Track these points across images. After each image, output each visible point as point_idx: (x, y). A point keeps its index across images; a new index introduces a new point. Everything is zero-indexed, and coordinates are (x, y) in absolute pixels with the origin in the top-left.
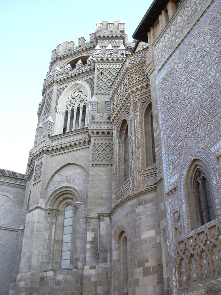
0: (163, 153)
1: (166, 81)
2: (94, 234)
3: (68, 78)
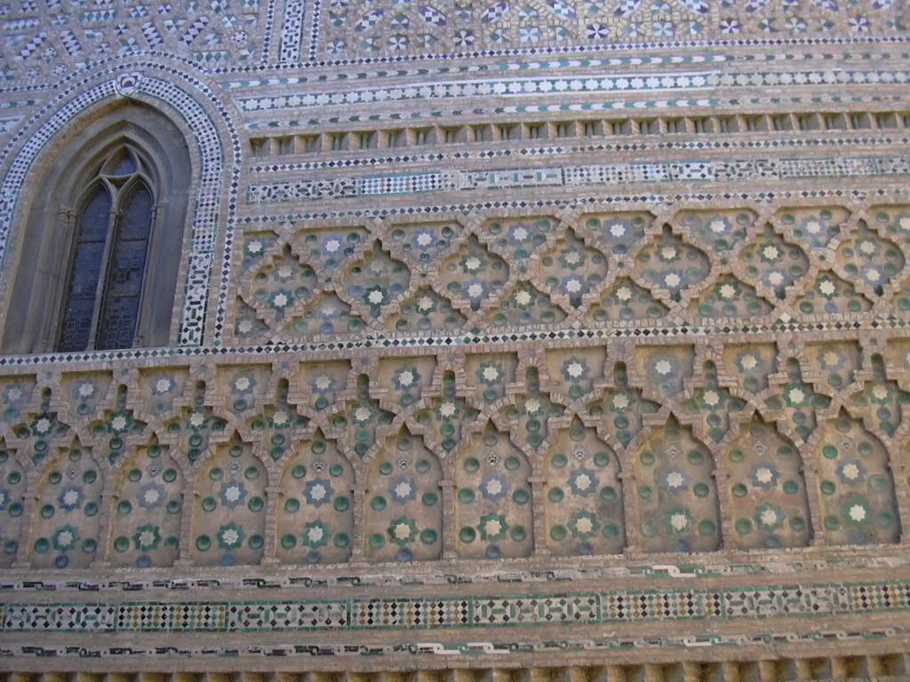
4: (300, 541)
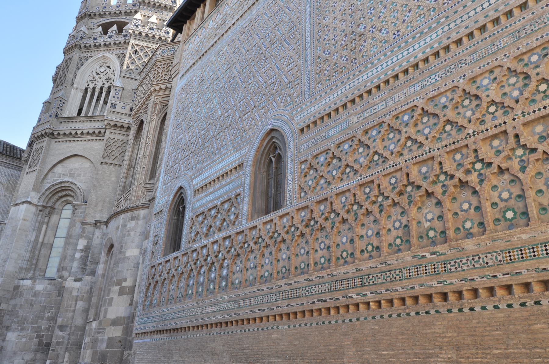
0: (162, 170)
2: (88, 242)
3: (95, 46)
4: (319, 263)
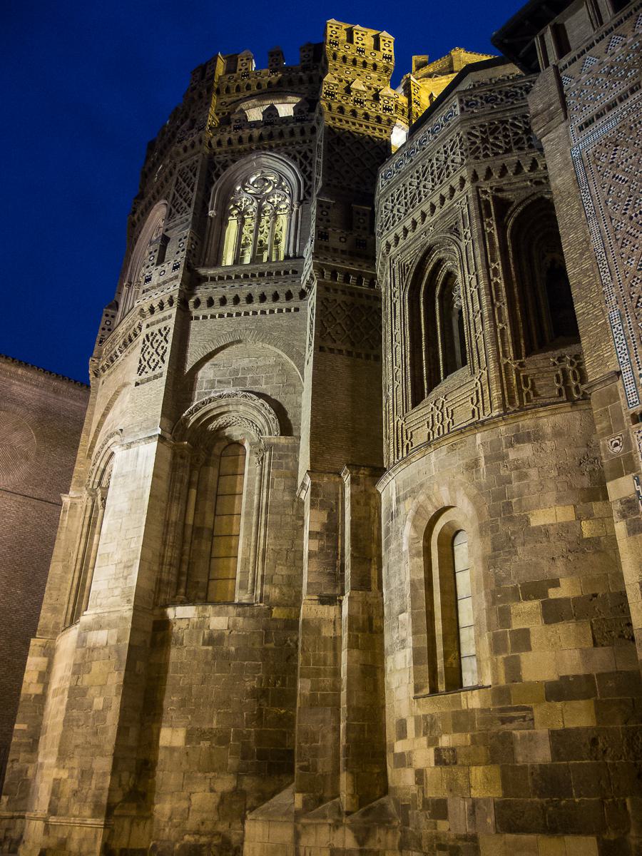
1: (617, 146)
2: (329, 516)
